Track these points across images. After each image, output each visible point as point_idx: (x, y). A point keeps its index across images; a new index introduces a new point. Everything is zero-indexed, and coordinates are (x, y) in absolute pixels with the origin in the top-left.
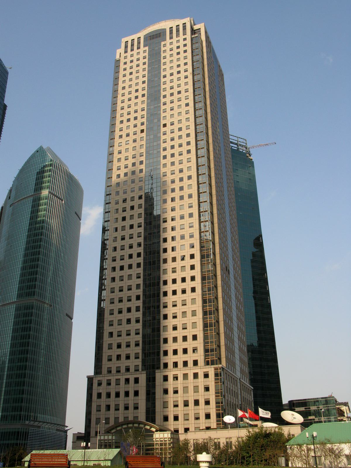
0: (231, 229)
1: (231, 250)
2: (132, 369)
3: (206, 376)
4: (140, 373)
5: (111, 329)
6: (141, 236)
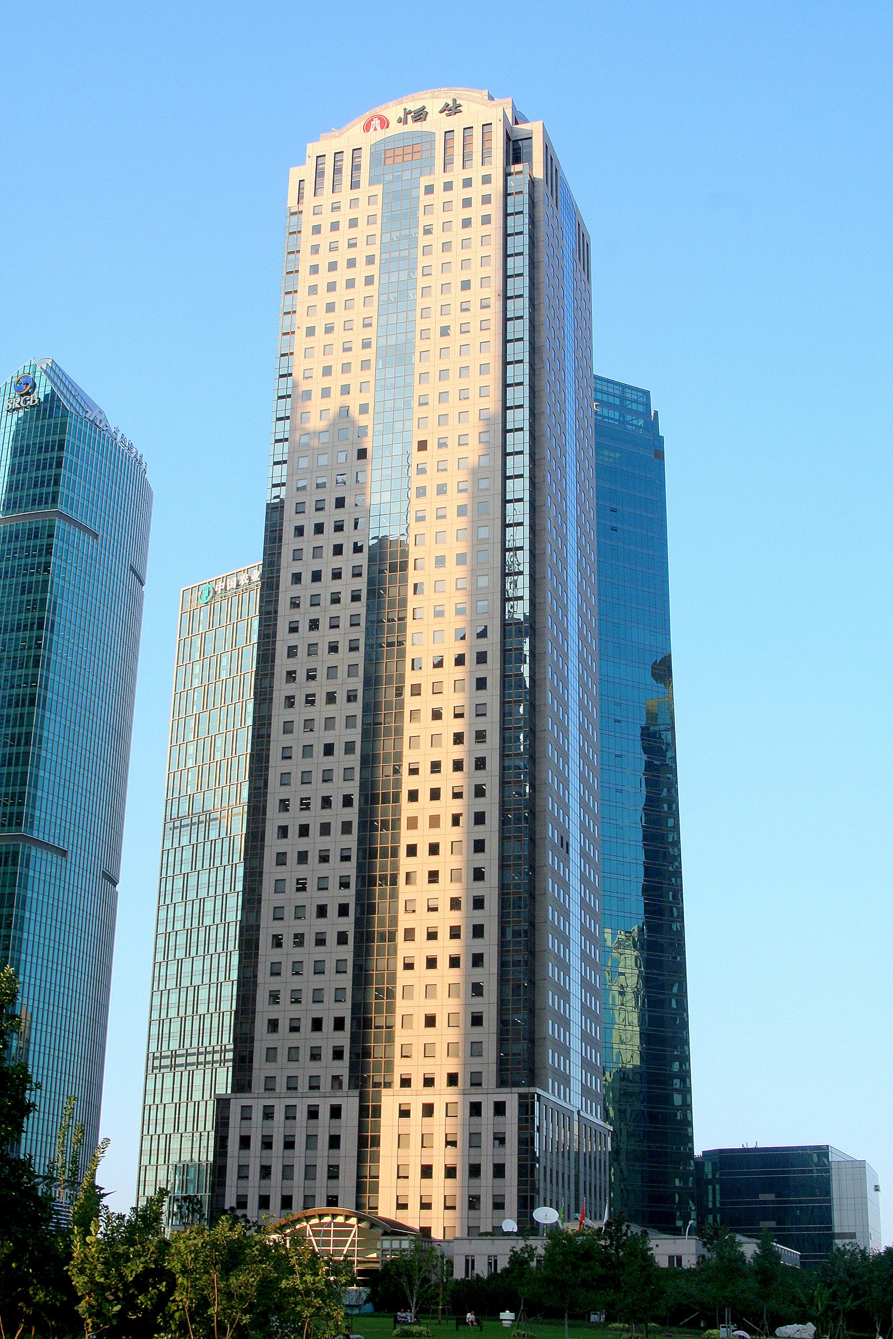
0: (578, 475)
1: (576, 662)
2: (326, 1084)
3: (500, 1109)
4: (345, 1094)
5: (274, 983)
6: (358, 624)
